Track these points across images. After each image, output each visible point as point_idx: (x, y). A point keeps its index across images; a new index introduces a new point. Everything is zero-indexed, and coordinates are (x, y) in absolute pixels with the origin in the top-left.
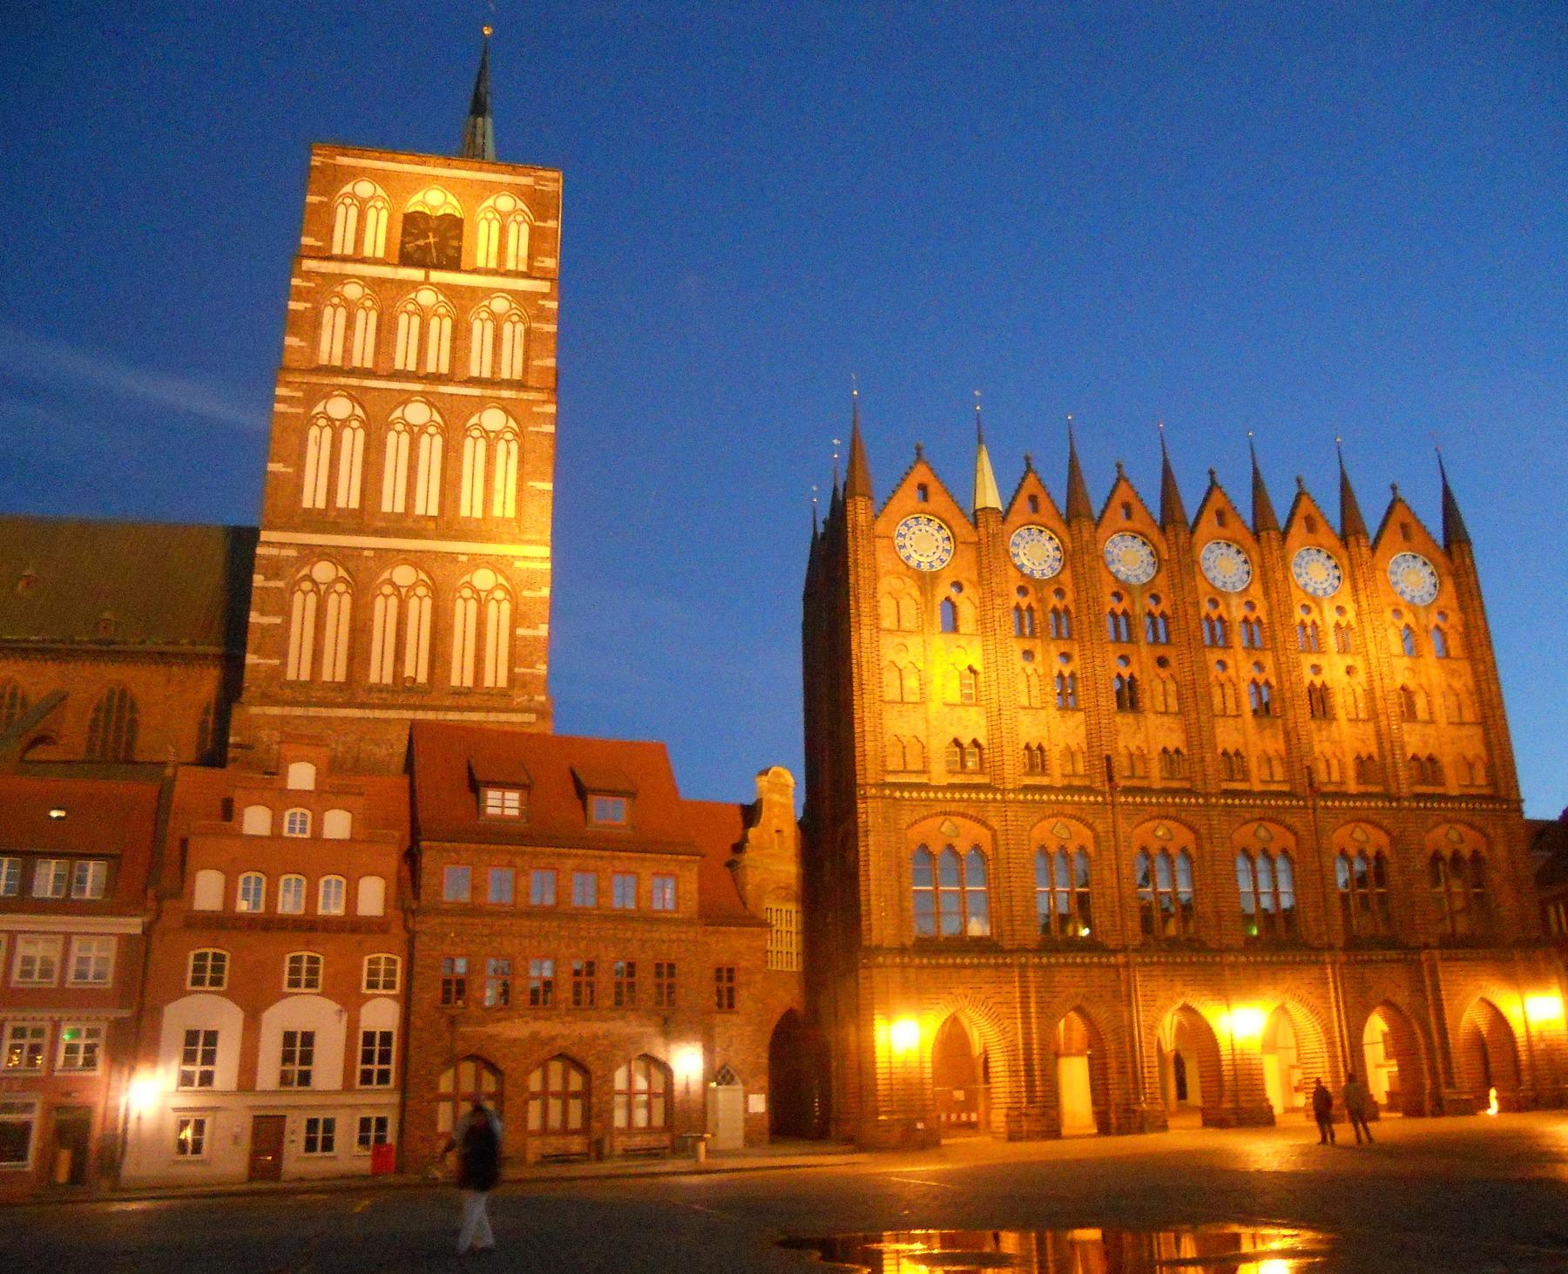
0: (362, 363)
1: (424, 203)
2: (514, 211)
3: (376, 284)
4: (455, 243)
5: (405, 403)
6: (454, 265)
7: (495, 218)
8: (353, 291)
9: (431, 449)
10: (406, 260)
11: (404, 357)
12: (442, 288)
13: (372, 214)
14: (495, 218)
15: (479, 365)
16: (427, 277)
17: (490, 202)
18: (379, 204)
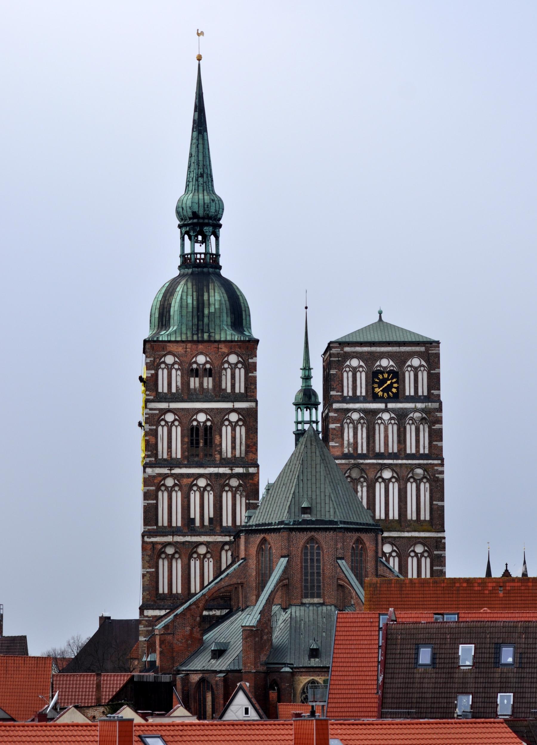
0: (362, 452)
1: (380, 366)
2: (421, 366)
3: (365, 411)
4: (395, 385)
5: (381, 470)
6: (396, 398)
7: (411, 370)
8: (355, 416)
9: (394, 488)
10: (375, 398)
11: (380, 447)
12: (393, 410)
13: (358, 374)
14: (411, 370)
15: (411, 449)
16: (386, 406)
17: (409, 363)
18: (361, 369)
